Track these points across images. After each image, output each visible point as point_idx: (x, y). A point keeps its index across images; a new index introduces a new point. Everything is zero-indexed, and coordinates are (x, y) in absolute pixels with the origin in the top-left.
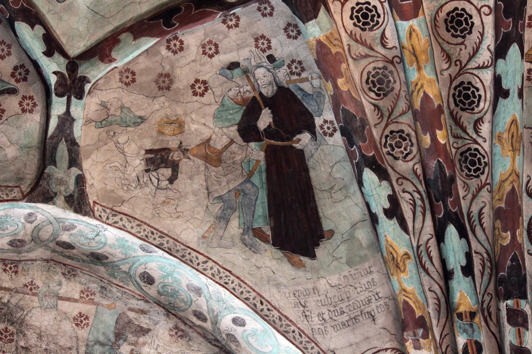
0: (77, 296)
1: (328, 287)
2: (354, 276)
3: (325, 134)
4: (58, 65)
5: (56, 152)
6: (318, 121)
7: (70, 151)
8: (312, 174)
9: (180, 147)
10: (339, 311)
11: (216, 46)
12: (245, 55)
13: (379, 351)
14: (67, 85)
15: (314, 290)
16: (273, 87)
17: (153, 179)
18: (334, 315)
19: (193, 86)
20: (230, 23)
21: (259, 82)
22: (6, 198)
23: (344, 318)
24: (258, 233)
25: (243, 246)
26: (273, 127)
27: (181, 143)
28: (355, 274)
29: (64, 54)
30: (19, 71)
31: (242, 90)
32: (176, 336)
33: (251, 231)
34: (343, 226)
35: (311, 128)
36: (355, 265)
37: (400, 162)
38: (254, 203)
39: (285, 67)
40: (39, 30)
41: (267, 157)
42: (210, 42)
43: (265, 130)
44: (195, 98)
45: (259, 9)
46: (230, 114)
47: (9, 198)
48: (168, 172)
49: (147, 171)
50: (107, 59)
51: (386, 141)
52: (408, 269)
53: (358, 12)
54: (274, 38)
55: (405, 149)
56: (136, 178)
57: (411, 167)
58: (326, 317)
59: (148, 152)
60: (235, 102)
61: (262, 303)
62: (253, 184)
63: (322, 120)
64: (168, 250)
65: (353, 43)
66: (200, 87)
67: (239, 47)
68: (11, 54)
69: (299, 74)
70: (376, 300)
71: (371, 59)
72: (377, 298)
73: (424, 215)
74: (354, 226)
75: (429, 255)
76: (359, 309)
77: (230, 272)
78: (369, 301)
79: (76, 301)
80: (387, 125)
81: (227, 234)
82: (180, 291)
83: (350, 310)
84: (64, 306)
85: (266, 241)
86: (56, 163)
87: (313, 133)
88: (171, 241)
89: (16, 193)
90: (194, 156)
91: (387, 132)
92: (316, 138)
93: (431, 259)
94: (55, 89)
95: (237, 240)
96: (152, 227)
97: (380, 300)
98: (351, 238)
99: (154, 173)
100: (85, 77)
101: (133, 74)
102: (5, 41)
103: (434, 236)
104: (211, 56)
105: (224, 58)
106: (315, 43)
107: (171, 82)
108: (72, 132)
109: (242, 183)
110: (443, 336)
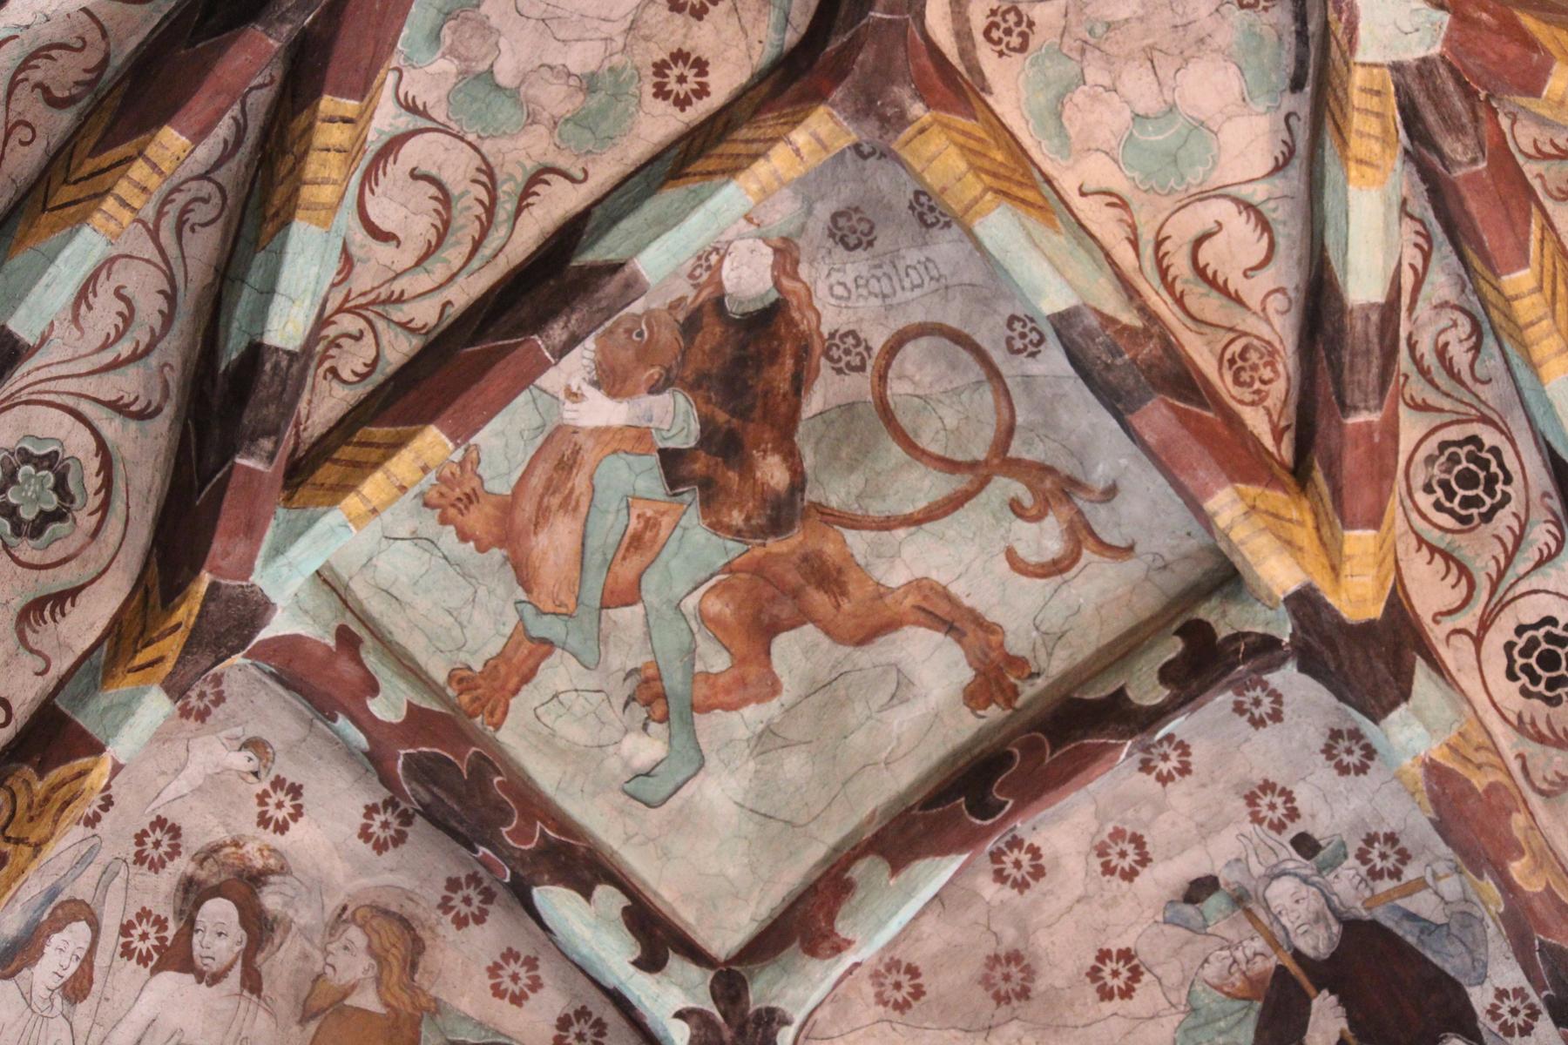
4: (687, 989)
6: (1480, 998)
11: (1138, 841)
12: (1229, 849)
16: (1328, 927)
19: (1094, 974)
20: (1164, 767)
21: (1284, 920)
29: (696, 954)
30: (575, 1029)
31: (1239, 954)
39: (1352, 861)
40: (609, 899)
42: (1118, 834)
44: (1107, 1007)
45: (1239, 709)
46: (1221, 1033)
50: (826, 945)
53: (1525, 653)
54: (1301, 783)
60: (1228, 994)
65: (1531, 748)
66: (1117, 974)
67: (1206, 831)
68: (541, 986)
69: (1396, 874)
100: (771, 1011)
101: (913, 972)
102: (515, 949)
104: (1129, 875)
105: (1169, 873)
106: (1419, 772)
107: (1029, 973)
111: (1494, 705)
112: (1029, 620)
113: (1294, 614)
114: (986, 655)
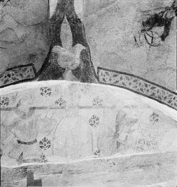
0: (91, 105)
5: (59, 32)
7: (72, 28)
17: (148, 37)
22: (20, 79)
32: (154, 121)
47: (24, 79)
49: (143, 31)
56: (134, 39)
64: (158, 99)
79: (90, 107)
84: (83, 112)
86: (61, 42)
88: (161, 89)
89: (29, 72)
99: (149, 32)
108: (73, 9)
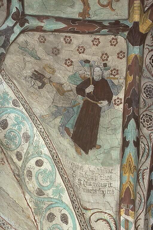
1: (88, 170)
2: (102, 170)
3: (115, 104)
6: (114, 97)
8: (101, 119)
9: (49, 78)
10: (89, 183)
11: (84, 49)
12: (94, 59)
13: (102, 212)
14: (18, 17)
15: (81, 167)
16: (100, 77)
17: (32, 82)
18: (86, 184)
19: (66, 60)
20: (95, 43)
21: (95, 73)
23: (90, 188)
24: (67, 130)
25: (58, 130)
26: (92, 94)
27: (51, 77)
28: (103, 170)
31: (86, 73)
33: (64, 127)
34: (107, 146)
35: (109, 100)
36: (105, 166)
37: (145, 129)
38: (71, 117)
39: (110, 71)
41: (84, 104)
42: (83, 47)
43: (88, 93)
44: (65, 65)
46: (76, 80)
48: (40, 84)
51: (143, 117)
52: (134, 174)
54: (111, 56)
55: (150, 124)
57: (149, 133)
58: (82, 182)
59: (35, 71)
61: (56, 157)
62: (73, 110)
63: (117, 97)
65: (146, 70)
66: (69, 62)
67: (94, 55)
69: (114, 76)
70: (109, 187)
71: (150, 81)
72: (110, 186)
73: (147, 157)
74: (112, 148)
75: (143, 176)
76: (99, 187)
77: (48, 136)
78: (105, 186)
80: (145, 111)
81: (53, 121)
82: (17, 137)
83: (94, 186)
85: (69, 135)
87: (110, 102)
90: (54, 85)
91: (145, 113)
92: (110, 105)
93: (143, 179)
94: (13, 15)
95: (57, 127)
96: (23, 96)
97: (111, 187)
98: (108, 153)
101: (45, 40)
103: (148, 169)
104: (80, 53)
105: (85, 56)
106: (134, 56)
107: (59, 53)
109: (69, 107)
110: (138, 219)
111: (145, 61)
112: (94, 10)
113: (134, 24)
114: (86, 11)
